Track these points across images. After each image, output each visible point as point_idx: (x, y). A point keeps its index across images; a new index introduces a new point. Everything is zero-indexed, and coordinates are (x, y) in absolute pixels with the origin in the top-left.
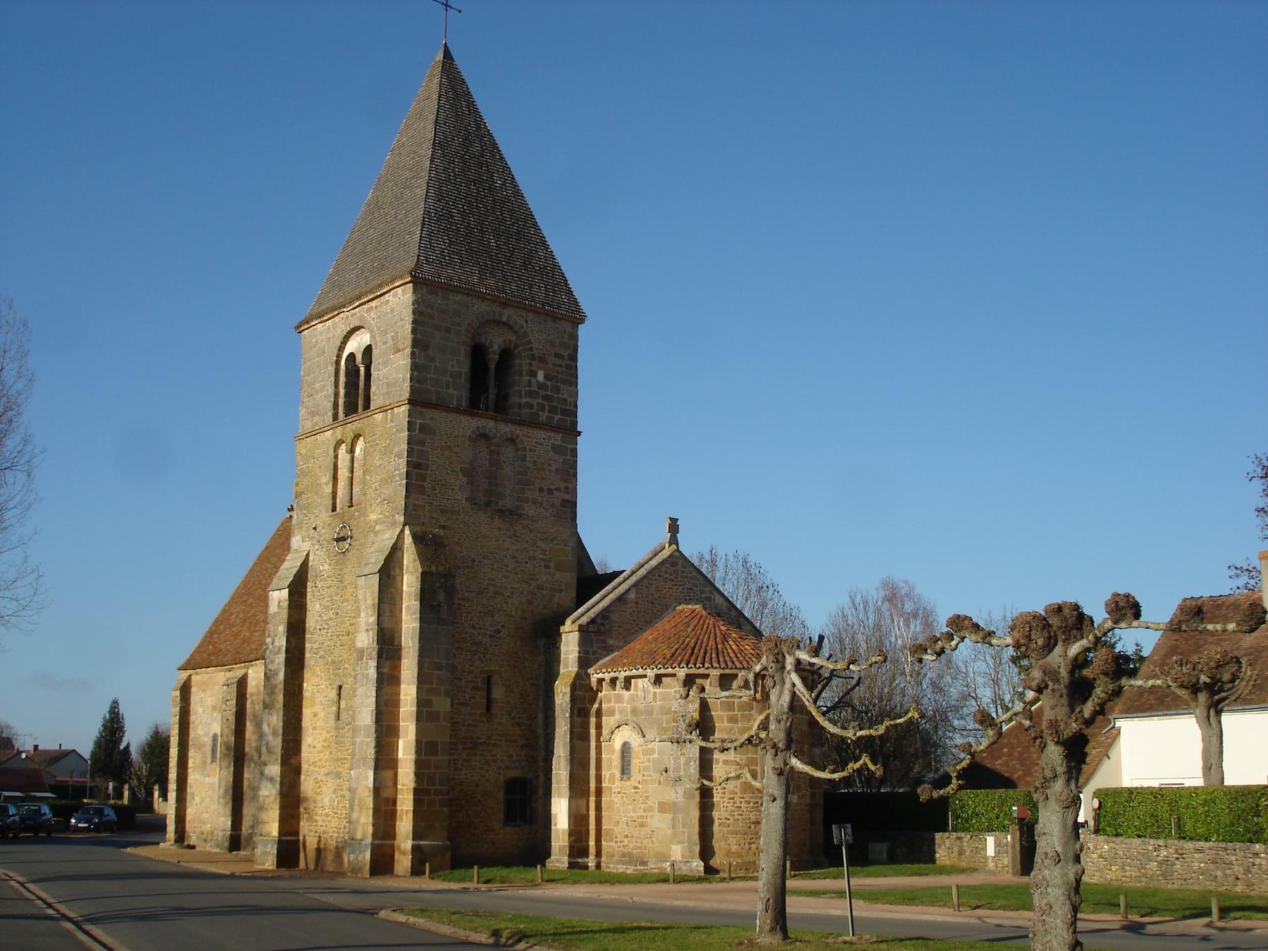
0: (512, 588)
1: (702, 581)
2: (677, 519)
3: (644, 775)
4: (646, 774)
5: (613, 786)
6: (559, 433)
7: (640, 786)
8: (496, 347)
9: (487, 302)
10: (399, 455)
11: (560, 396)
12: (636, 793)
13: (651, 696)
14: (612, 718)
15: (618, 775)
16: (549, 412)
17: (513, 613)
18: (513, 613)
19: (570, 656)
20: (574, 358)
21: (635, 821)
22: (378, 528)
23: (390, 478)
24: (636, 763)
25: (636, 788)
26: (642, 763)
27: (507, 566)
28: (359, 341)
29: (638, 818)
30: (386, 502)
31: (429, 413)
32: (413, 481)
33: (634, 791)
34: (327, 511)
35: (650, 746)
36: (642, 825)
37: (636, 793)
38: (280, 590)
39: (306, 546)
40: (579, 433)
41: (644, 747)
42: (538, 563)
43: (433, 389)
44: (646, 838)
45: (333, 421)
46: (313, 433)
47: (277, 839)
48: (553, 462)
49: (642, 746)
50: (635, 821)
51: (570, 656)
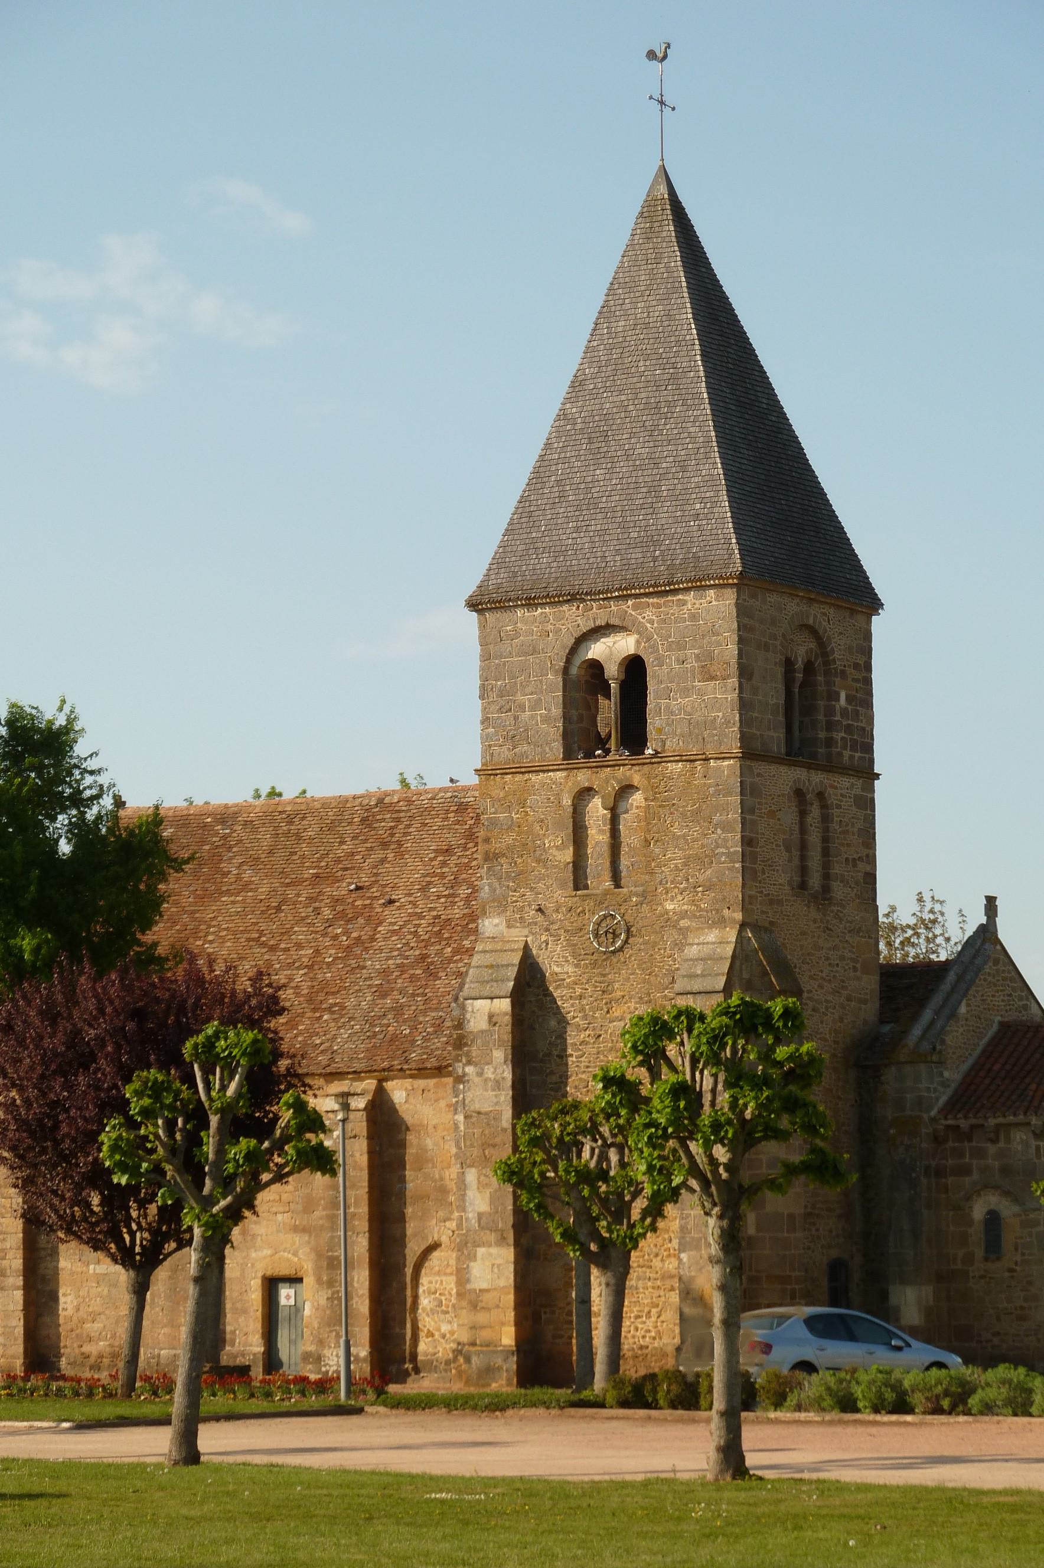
0: (826, 1001)
1: (1019, 984)
2: (996, 898)
3: (1023, 1254)
4: (1027, 1252)
5: (970, 1269)
6: (859, 777)
7: (1018, 1268)
8: (800, 659)
9: (796, 600)
10: (726, 827)
11: (859, 724)
12: (1012, 1277)
13: (1033, 1150)
14: (967, 1179)
15: (979, 1253)
16: (851, 750)
17: (828, 1036)
18: (828, 1036)
19: (908, 1096)
20: (868, 668)
21: (1012, 1313)
22: (684, 923)
23: (706, 856)
24: (1009, 1238)
25: (1011, 1270)
26: (1021, 1238)
27: (822, 971)
28: (611, 644)
29: (1016, 1309)
30: (700, 889)
31: (760, 767)
32: (748, 865)
33: (1007, 1274)
34: (563, 886)
35: (1032, 1216)
36: (1022, 1318)
37: (1012, 1277)
38: (492, 998)
39: (518, 936)
40: (877, 776)
41: (1023, 1217)
42: (847, 964)
43: (758, 733)
44: (1027, 1336)
45: (564, 759)
46: (523, 770)
47: (514, 1349)
48: (855, 821)
49: (1020, 1215)
50: (1012, 1313)
51: (908, 1096)
